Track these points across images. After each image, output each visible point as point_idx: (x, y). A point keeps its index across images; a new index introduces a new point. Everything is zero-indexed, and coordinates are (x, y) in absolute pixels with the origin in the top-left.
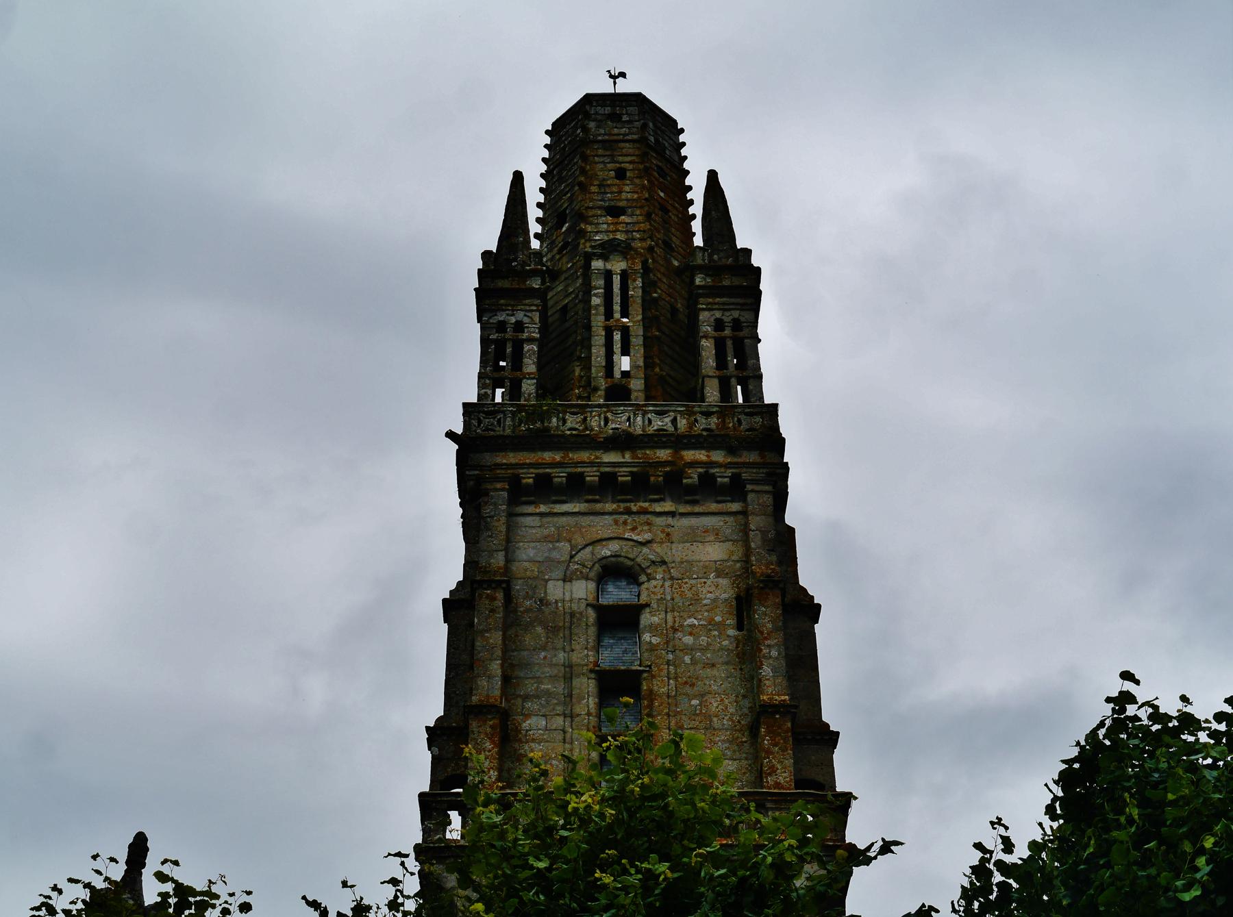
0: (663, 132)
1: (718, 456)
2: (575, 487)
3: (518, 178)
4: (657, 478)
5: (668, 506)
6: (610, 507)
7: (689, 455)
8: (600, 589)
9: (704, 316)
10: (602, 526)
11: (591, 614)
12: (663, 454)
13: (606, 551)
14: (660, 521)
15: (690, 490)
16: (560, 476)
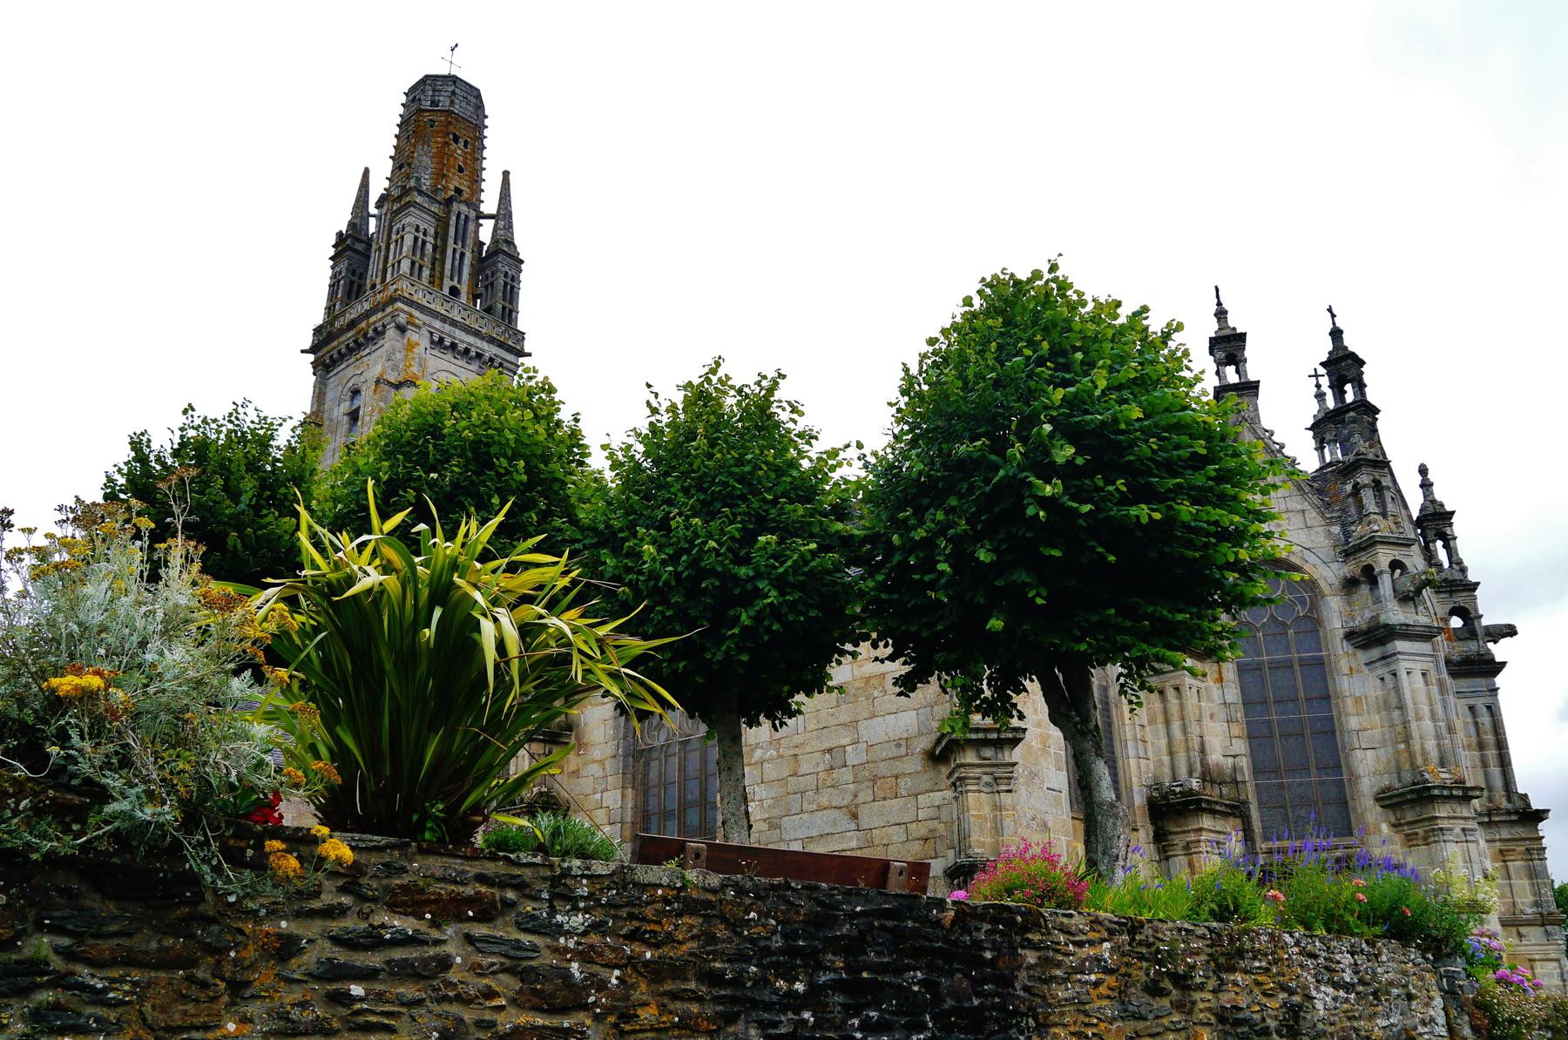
0: (440, 91)
1: (380, 315)
2: (342, 357)
3: (366, 172)
4: (361, 340)
5: (367, 351)
6: (353, 359)
7: (372, 319)
8: (352, 404)
9: (395, 229)
10: (351, 371)
11: (346, 418)
12: (363, 324)
13: (350, 384)
14: (365, 359)
15: (372, 339)
16: (335, 352)
